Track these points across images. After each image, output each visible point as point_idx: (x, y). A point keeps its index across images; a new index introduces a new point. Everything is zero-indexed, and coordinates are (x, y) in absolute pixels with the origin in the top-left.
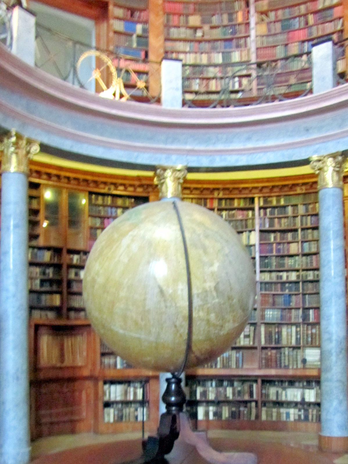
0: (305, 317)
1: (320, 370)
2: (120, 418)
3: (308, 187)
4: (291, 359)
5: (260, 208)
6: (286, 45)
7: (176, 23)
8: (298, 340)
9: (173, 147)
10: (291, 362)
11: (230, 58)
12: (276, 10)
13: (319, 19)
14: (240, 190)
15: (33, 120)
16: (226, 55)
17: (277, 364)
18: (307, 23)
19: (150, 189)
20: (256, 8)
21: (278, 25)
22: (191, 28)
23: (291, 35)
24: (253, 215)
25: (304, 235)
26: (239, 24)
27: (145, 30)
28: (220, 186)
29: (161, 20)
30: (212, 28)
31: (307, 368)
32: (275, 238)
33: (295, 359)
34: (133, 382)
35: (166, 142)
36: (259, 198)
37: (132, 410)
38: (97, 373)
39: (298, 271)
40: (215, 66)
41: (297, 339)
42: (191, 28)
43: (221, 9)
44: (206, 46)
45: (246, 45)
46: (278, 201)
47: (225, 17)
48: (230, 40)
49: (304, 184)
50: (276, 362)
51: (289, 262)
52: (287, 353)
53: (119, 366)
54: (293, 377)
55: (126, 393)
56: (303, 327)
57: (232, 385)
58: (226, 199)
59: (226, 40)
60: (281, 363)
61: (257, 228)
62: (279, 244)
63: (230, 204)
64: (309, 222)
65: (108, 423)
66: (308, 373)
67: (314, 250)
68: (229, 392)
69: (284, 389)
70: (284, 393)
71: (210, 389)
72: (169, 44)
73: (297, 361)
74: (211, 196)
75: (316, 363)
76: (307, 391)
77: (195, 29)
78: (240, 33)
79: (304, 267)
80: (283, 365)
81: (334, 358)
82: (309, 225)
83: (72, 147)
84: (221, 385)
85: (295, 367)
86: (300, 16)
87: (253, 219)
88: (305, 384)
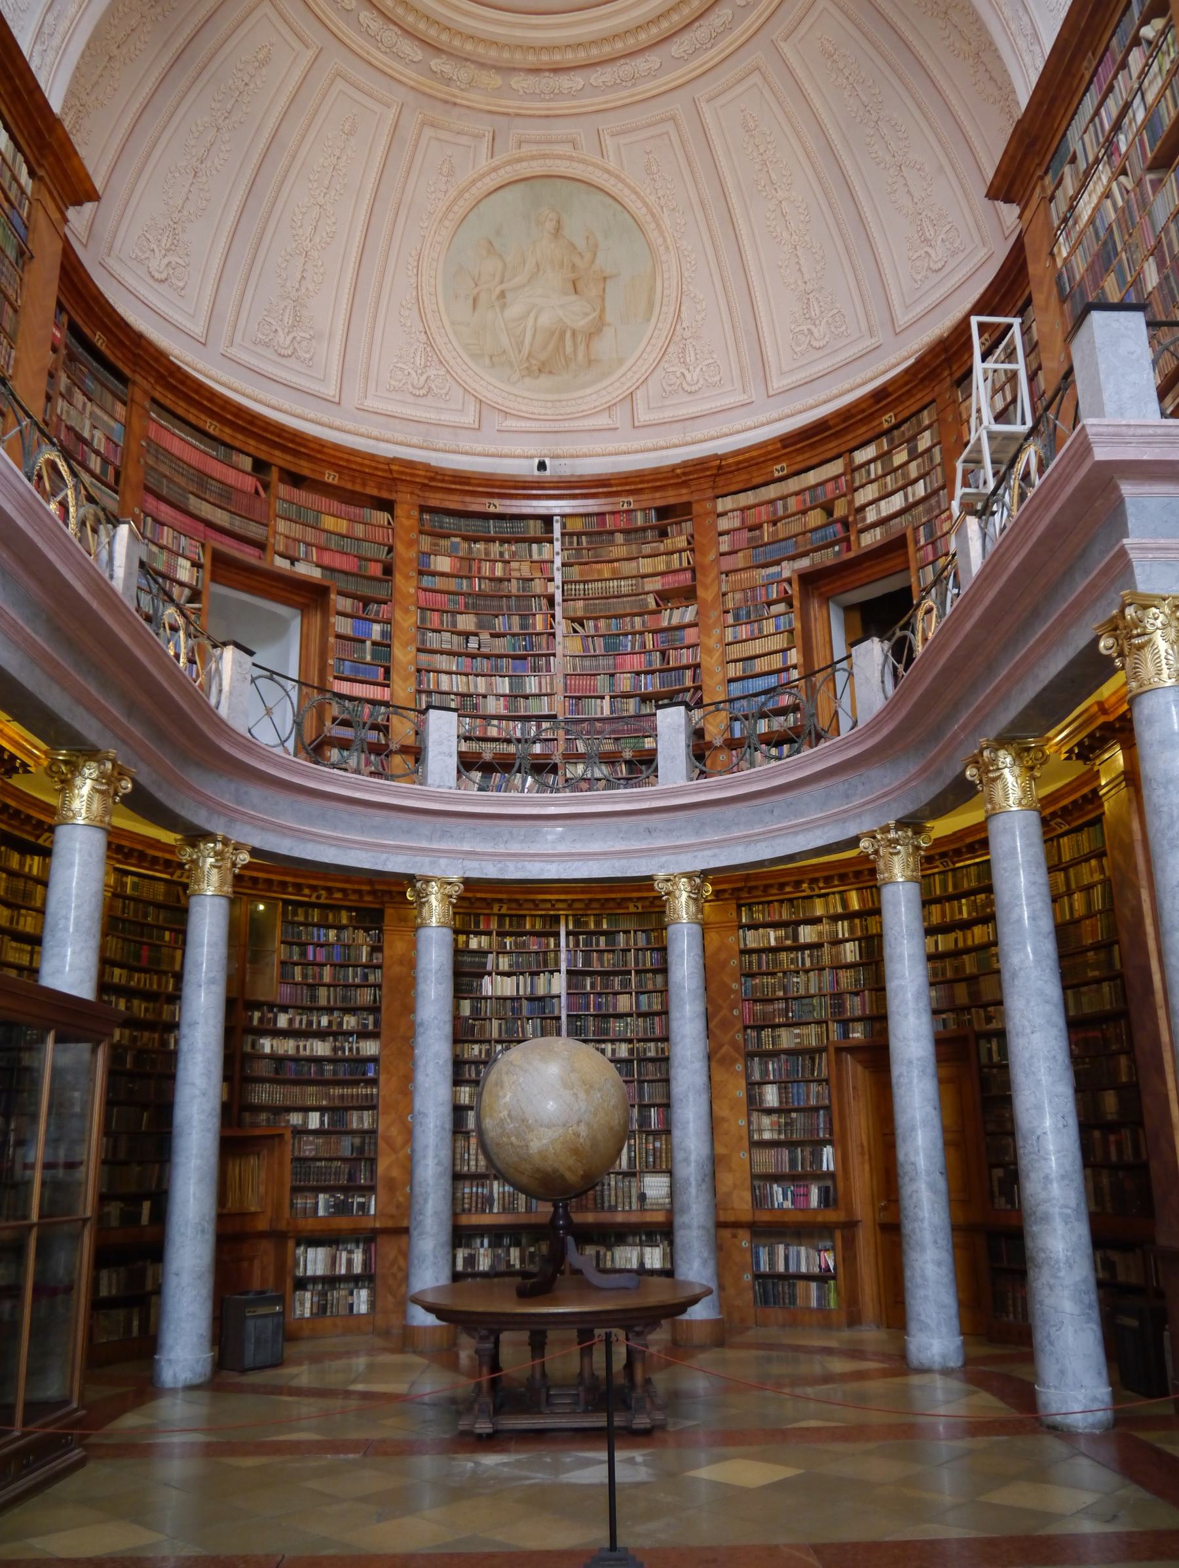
0: (644, 1121)
1: (670, 1212)
2: (321, 1309)
3: (647, 903)
4: (620, 1194)
5: (568, 934)
6: (612, 675)
7: (436, 626)
8: (631, 1160)
9: (443, 846)
10: (620, 1200)
11: (522, 685)
12: (596, 619)
13: (663, 642)
14: (536, 904)
15: (244, 814)
16: (516, 679)
17: (596, 1203)
19: (386, 899)
20: (564, 611)
21: (600, 642)
22: (459, 634)
23: (619, 659)
24: (558, 945)
25: (641, 980)
26: (538, 634)
27: (384, 634)
28: (504, 896)
29: (412, 620)
30: (493, 636)
31: (646, 1210)
32: (593, 986)
33: (627, 1194)
34: (345, 1242)
35: (430, 839)
36: (567, 916)
37: (343, 1293)
38: (283, 1226)
39: (630, 1041)
40: (498, 696)
41: (629, 1158)
42: (459, 634)
43: (509, 608)
44: (484, 665)
45: (549, 670)
46: (598, 923)
47: (516, 620)
48: (524, 657)
49: (639, 899)
50: (595, 1200)
51: (617, 1026)
52: (613, 1183)
53: (321, 1213)
54: (622, 1225)
55: (333, 1262)
56: (640, 1139)
57: (517, 1244)
58: (511, 916)
59: (515, 657)
60: (603, 1202)
61: (563, 967)
62: (600, 994)
63: (519, 925)
64: (649, 960)
65: (302, 1318)
66: (649, 1218)
67: (657, 1007)
68: (515, 1253)
69: (609, 1247)
70: (609, 1254)
71: (482, 1251)
72: (423, 657)
73: (630, 1197)
74: (486, 911)
75: (661, 1201)
76: (648, 1250)
77: (467, 635)
78: (540, 648)
79: (641, 1035)
80: (606, 1205)
81: (693, 1190)
82: (648, 965)
83: (291, 849)
84: (500, 1245)
85: (627, 1208)
86: (634, 634)
87: (557, 951)
88: (644, 1238)
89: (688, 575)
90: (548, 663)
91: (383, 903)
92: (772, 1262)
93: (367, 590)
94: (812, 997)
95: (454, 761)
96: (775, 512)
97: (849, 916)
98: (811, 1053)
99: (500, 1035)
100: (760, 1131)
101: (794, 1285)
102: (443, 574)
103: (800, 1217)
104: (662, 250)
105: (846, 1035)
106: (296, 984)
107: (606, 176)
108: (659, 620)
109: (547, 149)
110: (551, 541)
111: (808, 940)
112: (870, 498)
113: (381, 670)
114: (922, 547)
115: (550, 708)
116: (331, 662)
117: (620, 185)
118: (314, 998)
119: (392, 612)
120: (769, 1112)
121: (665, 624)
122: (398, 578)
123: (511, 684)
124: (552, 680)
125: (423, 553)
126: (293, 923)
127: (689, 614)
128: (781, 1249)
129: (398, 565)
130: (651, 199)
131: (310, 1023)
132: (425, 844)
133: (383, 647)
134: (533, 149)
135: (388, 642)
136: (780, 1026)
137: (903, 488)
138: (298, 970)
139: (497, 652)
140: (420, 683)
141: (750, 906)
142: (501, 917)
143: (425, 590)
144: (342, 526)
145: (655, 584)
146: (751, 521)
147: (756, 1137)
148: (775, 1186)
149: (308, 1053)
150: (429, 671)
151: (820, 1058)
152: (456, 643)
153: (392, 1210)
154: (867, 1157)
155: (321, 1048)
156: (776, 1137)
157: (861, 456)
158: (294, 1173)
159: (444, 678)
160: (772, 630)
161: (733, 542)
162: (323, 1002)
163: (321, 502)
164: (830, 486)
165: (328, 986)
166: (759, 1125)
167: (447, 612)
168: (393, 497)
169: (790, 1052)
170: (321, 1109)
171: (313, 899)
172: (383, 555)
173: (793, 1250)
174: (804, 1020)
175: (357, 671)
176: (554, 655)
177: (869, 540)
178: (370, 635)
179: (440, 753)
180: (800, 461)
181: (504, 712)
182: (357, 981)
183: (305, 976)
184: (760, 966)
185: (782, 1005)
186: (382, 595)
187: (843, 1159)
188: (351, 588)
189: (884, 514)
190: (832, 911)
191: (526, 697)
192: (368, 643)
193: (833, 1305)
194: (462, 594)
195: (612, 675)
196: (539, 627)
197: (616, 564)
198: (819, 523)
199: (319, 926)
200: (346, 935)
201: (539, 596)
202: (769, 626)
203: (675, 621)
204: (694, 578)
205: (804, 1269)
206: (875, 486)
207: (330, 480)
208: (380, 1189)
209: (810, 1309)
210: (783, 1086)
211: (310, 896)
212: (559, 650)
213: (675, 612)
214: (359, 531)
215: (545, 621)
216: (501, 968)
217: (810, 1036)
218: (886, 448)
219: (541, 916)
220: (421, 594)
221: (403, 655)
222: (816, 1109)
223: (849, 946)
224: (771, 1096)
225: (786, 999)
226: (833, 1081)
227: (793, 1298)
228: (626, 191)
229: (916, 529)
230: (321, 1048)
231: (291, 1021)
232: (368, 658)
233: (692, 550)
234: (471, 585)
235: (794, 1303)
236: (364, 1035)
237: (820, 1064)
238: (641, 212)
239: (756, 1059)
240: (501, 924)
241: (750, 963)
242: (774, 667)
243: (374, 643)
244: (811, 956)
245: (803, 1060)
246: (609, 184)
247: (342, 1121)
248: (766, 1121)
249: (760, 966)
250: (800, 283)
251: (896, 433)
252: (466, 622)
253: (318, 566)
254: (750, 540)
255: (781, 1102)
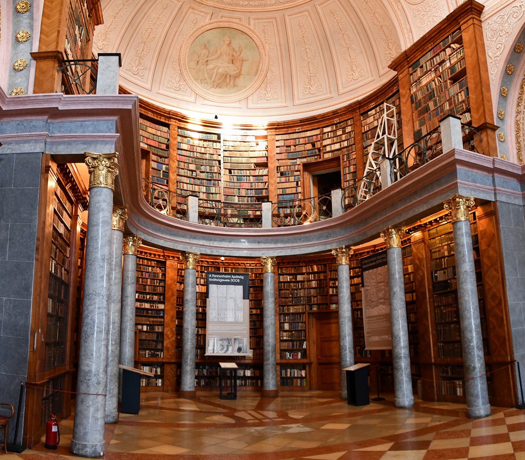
2: (148, 384)
7: (183, 167)
18: (249, 180)
20: (224, 166)
21: (235, 178)
22: (190, 170)
23: (242, 184)
26: (215, 173)
30: (201, 172)
42: (190, 170)
44: (198, 182)
48: (210, 180)
53: (147, 356)
59: (207, 180)
72: (179, 177)
77: (192, 171)
86: (247, 176)
89: (265, 159)
90: (218, 183)
91: (166, 259)
92: (286, 374)
93: (161, 153)
94: (301, 297)
95: (197, 214)
96: (296, 142)
97: (314, 273)
98: (300, 314)
99: (201, 304)
100: (283, 337)
101: (293, 380)
102: (185, 150)
103: (295, 361)
104: (264, 55)
105: (311, 309)
106: (140, 284)
107: (249, 30)
108: (255, 173)
109: (230, 20)
110: (220, 142)
111: (300, 280)
112: (328, 143)
113: (166, 181)
114: (345, 162)
115: (220, 198)
116: (150, 177)
117: (253, 34)
118: (145, 289)
119: (169, 161)
120: (286, 331)
121: (257, 174)
122: (171, 150)
123: (206, 189)
124: (219, 189)
125: (179, 142)
126: (139, 264)
127: (264, 172)
128: (289, 370)
129: (171, 145)
130: (263, 40)
131: (144, 297)
132: (188, 241)
133: (166, 173)
134: (226, 19)
135: (168, 171)
136: (290, 305)
137: (340, 142)
138: (141, 279)
139: (202, 178)
140: (177, 186)
141: (281, 268)
142: (202, 266)
143: (179, 155)
144: (154, 131)
145: (255, 161)
146: (286, 144)
147: (281, 338)
148: (287, 353)
149: (143, 307)
150: (180, 182)
151: (303, 316)
152: (189, 174)
153: (169, 357)
154: (315, 344)
155: (147, 306)
156: (288, 338)
157: (326, 130)
158: (139, 344)
159: (185, 185)
160: (293, 180)
161: (281, 150)
162: (147, 291)
163: (148, 123)
164: (315, 137)
165: (149, 285)
166: (283, 335)
167: (186, 163)
168: (170, 123)
169: (292, 314)
170: (147, 325)
171: (145, 257)
172: (166, 141)
173: (293, 371)
174: (298, 304)
175: (158, 180)
176: (220, 180)
177: (327, 156)
178: (162, 169)
179: (193, 211)
180: (305, 128)
181: (205, 198)
182: (158, 284)
183: (142, 282)
184: (284, 287)
185: (291, 299)
186: (166, 155)
187: (308, 345)
188: (156, 152)
189: (333, 149)
190: (308, 271)
191: (212, 194)
192: (162, 171)
193: (305, 385)
194: (191, 157)
195: (239, 189)
196: (216, 171)
197: (241, 152)
198: (310, 148)
199: (146, 266)
200: (154, 269)
201: (216, 160)
202: (292, 179)
203: (260, 174)
204: (267, 160)
205: (296, 375)
206: (330, 140)
207: (150, 116)
208: (165, 351)
209: (298, 386)
210: (290, 324)
211: (144, 256)
212: (222, 179)
213: (260, 170)
214: (159, 133)
215: (218, 168)
216: (201, 283)
217: (300, 309)
218: (335, 129)
219: (214, 267)
220: (178, 156)
221: (173, 176)
222: (301, 331)
223: (314, 282)
224: (287, 326)
225: (292, 298)
226: (307, 322)
227: (292, 384)
228: (255, 36)
229: (343, 156)
230: (147, 306)
231: (138, 296)
232: (162, 176)
233: (267, 151)
234: (194, 155)
235: (293, 385)
236: (160, 302)
237: (303, 317)
238: (258, 43)
239: (282, 315)
240: (201, 269)
241: (281, 286)
242: (293, 192)
243: (163, 172)
244: (301, 285)
245: (297, 316)
246: (249, 33)
247: (153, 329)
248: (285, 334)
249: (284, 287)
250: (309, 73)
251: (338, 125)
252: (192, 167)
253: (146, 144)
254: (286, 150)
255: (290, 328)
